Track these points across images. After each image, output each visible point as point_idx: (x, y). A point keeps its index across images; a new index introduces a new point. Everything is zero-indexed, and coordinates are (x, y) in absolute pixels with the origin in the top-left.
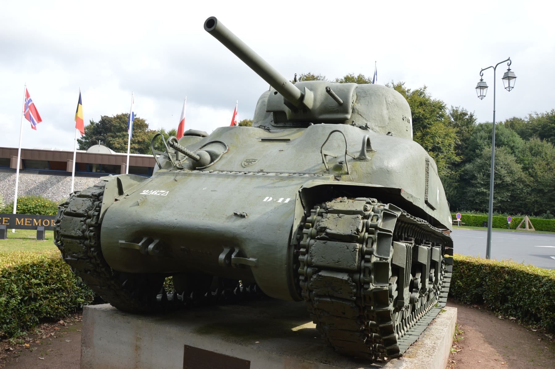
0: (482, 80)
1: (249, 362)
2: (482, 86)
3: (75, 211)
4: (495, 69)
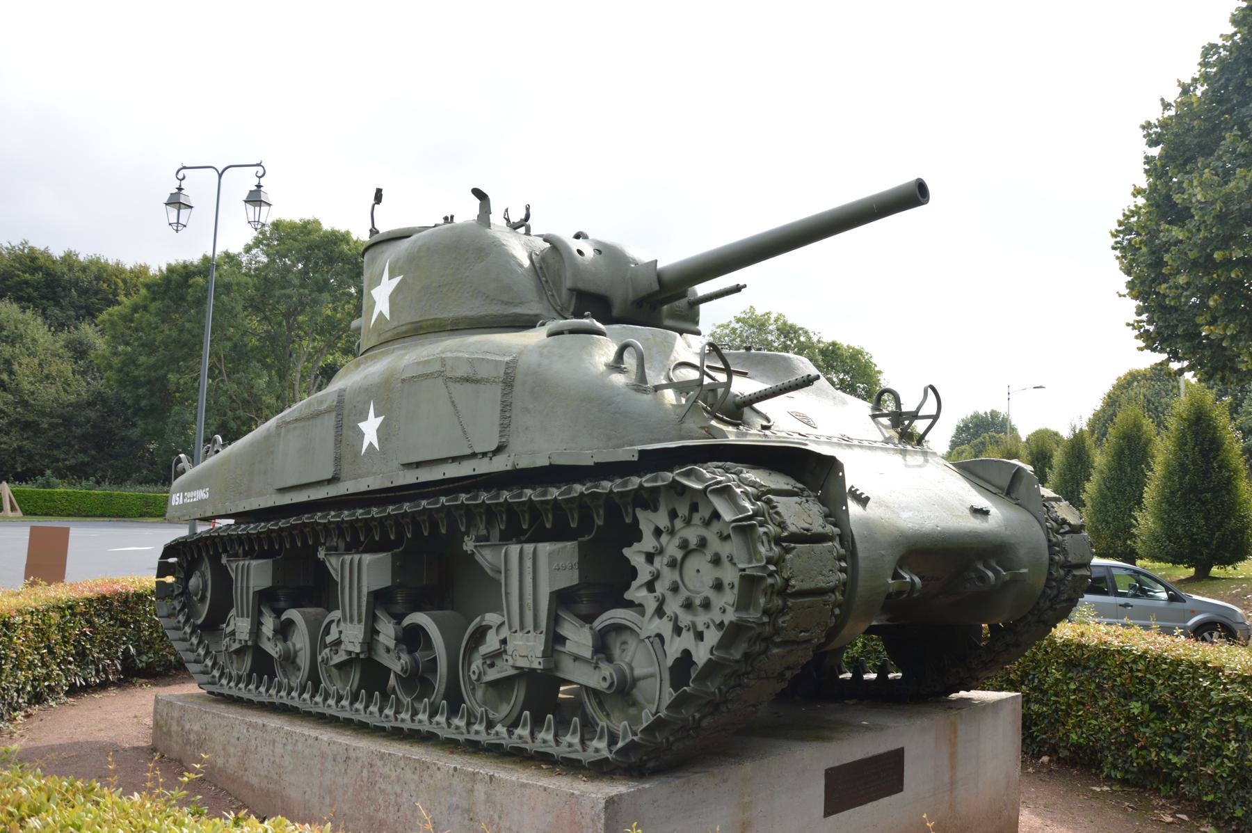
0: (180, 189)
1: (902, 749)
2: (176, 201)
3: (808, 530)
4: (220, 176)
